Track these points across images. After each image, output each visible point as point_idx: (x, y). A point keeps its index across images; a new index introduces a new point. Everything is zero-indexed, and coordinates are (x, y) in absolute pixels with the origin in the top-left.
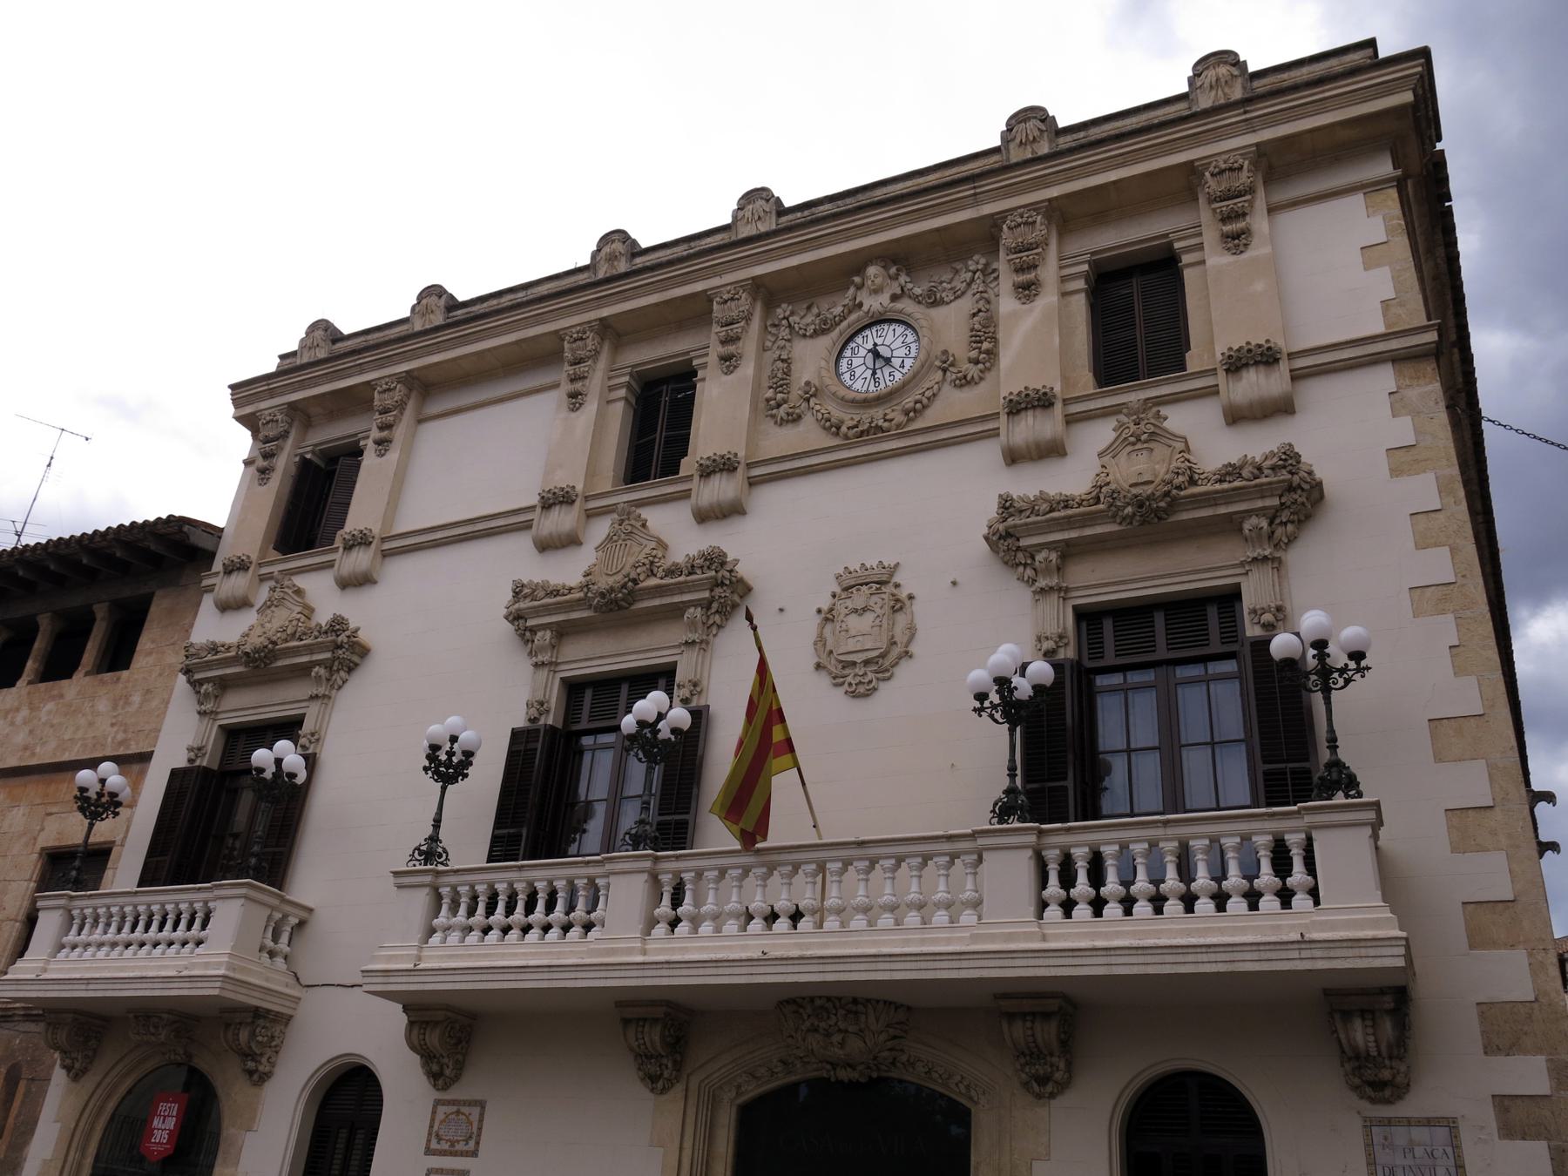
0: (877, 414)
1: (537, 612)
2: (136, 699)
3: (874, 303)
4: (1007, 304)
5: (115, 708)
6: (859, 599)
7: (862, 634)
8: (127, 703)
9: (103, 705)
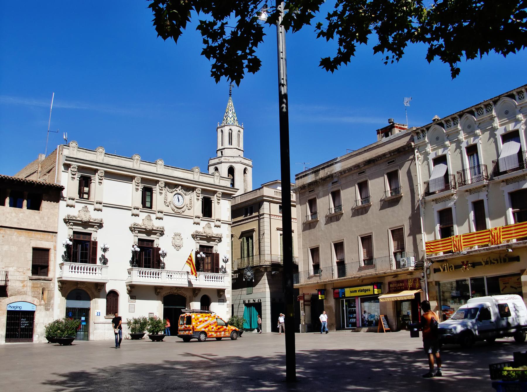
0: (179, 211)
1: (137, 228)
2: (46, 218)
3: (179, 192)
4: (196, 200)
5: (41, 219)
6: (178, 237)
7: (178, 243)
8: (43, 219)
9: (37, 218)
